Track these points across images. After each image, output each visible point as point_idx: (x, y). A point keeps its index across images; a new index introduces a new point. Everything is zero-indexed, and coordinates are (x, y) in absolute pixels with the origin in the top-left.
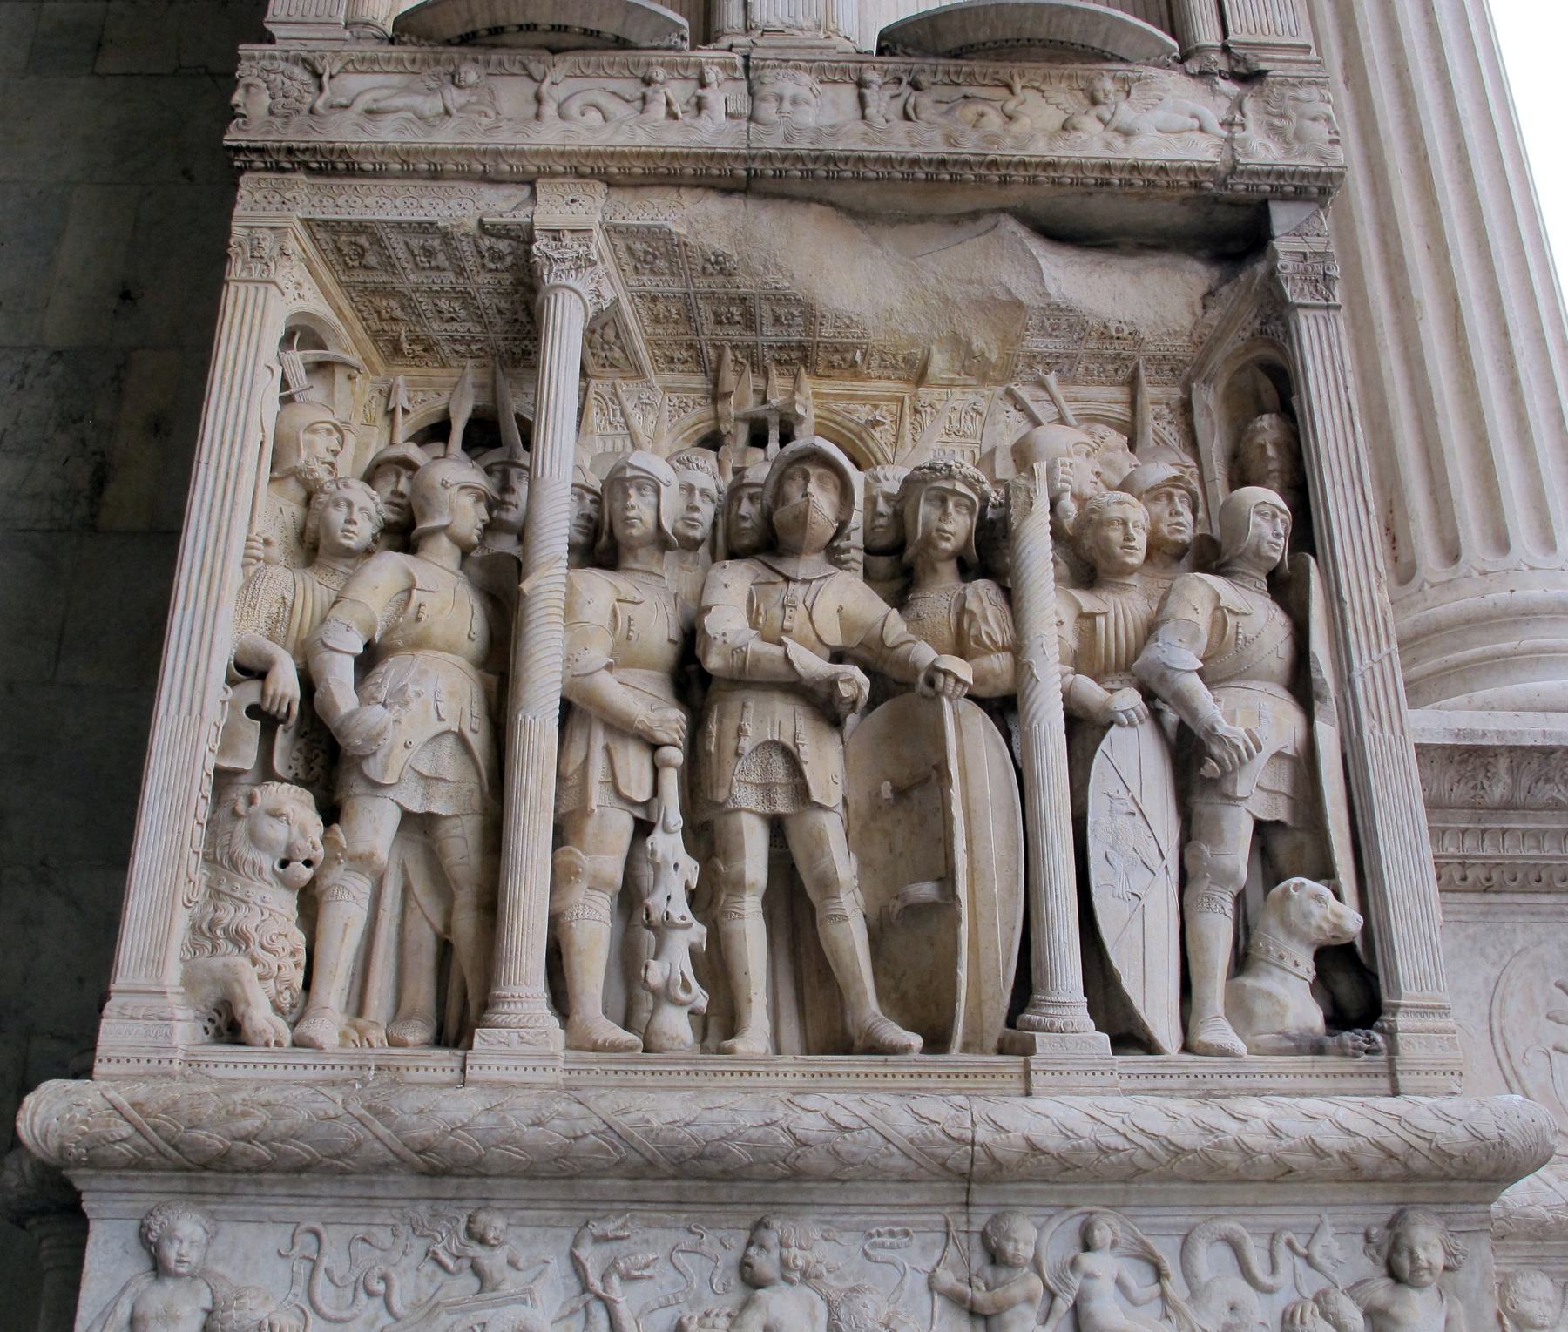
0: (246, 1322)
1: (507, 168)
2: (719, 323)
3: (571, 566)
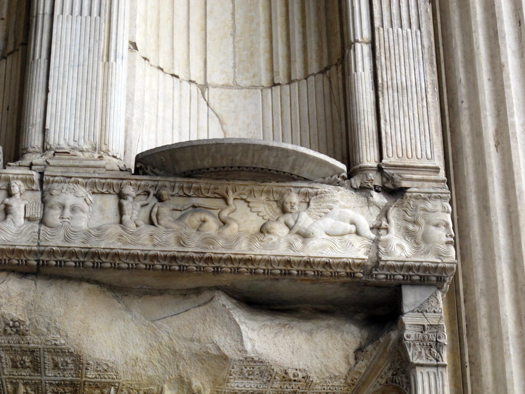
2: (15, 367)
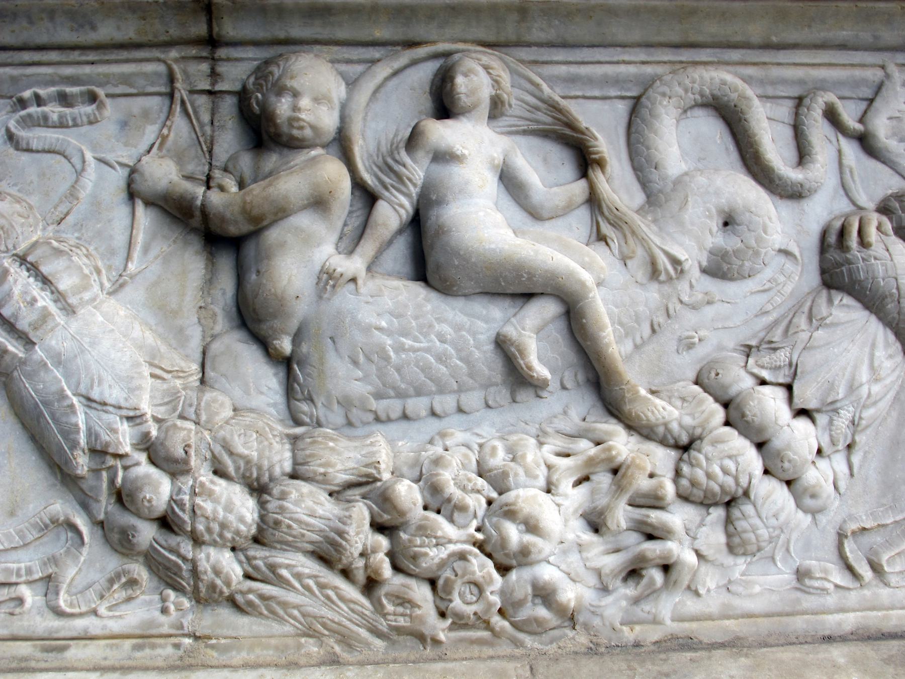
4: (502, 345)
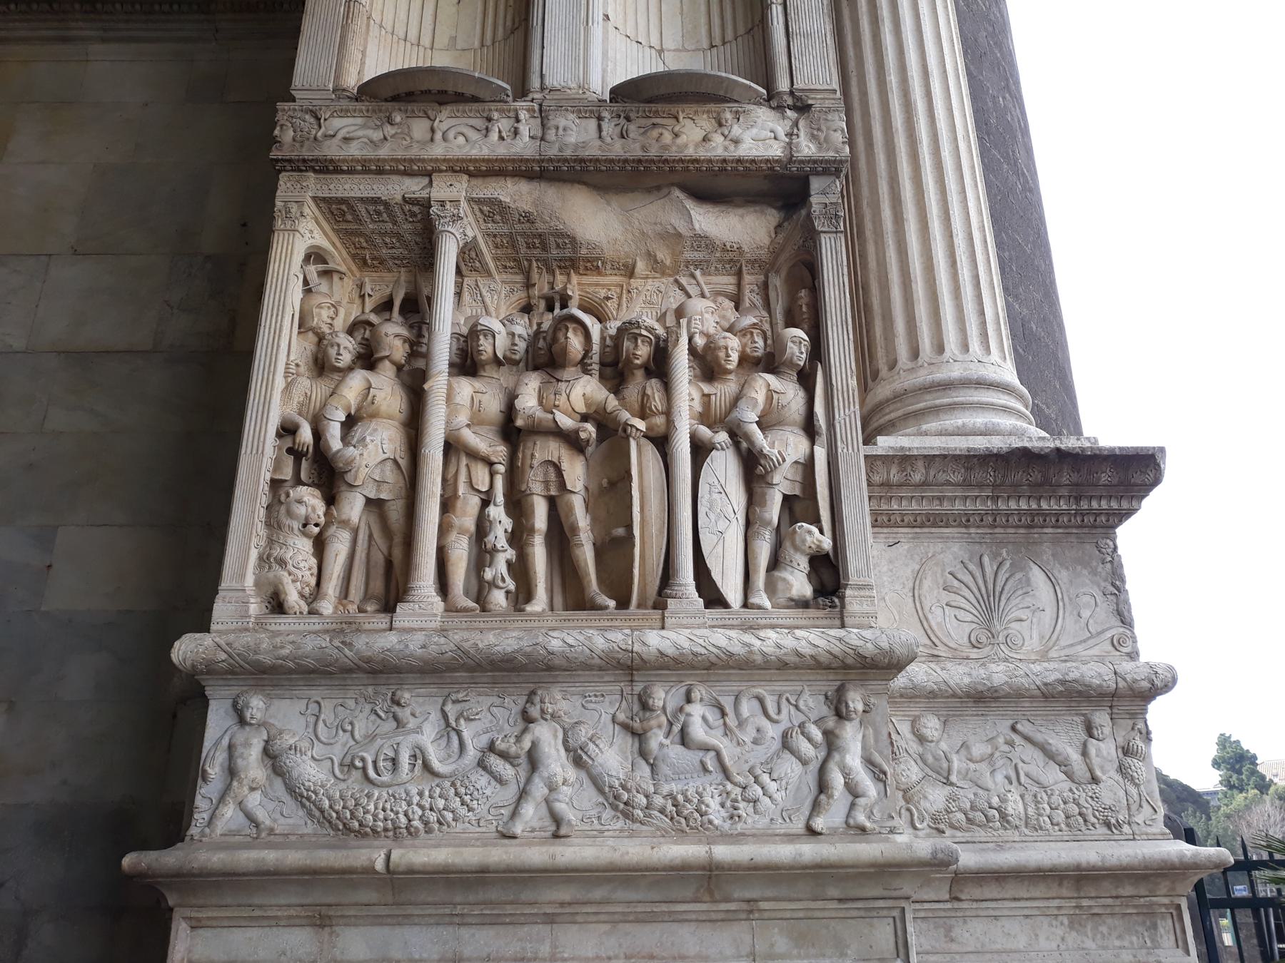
0: (284, 746)
1: (417, 168)
3: (450, 374)
4: (702, 762)
